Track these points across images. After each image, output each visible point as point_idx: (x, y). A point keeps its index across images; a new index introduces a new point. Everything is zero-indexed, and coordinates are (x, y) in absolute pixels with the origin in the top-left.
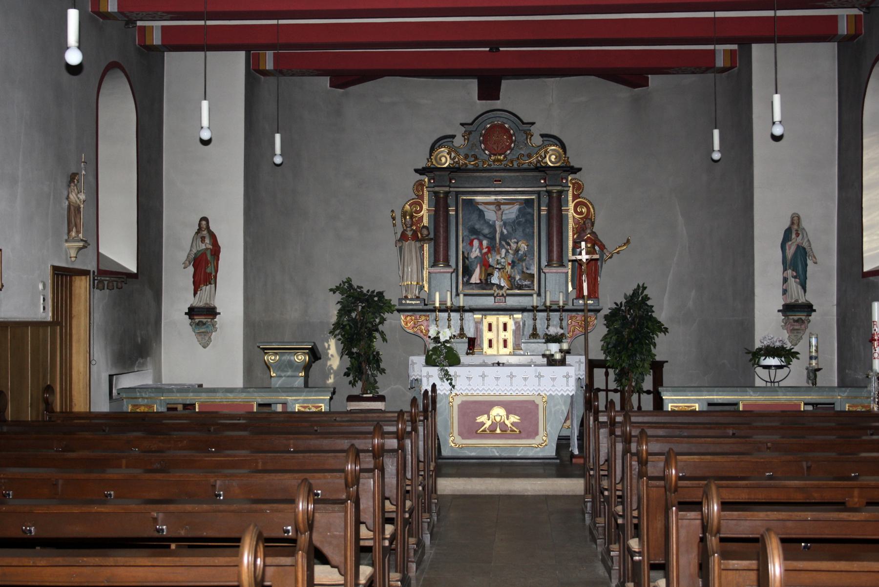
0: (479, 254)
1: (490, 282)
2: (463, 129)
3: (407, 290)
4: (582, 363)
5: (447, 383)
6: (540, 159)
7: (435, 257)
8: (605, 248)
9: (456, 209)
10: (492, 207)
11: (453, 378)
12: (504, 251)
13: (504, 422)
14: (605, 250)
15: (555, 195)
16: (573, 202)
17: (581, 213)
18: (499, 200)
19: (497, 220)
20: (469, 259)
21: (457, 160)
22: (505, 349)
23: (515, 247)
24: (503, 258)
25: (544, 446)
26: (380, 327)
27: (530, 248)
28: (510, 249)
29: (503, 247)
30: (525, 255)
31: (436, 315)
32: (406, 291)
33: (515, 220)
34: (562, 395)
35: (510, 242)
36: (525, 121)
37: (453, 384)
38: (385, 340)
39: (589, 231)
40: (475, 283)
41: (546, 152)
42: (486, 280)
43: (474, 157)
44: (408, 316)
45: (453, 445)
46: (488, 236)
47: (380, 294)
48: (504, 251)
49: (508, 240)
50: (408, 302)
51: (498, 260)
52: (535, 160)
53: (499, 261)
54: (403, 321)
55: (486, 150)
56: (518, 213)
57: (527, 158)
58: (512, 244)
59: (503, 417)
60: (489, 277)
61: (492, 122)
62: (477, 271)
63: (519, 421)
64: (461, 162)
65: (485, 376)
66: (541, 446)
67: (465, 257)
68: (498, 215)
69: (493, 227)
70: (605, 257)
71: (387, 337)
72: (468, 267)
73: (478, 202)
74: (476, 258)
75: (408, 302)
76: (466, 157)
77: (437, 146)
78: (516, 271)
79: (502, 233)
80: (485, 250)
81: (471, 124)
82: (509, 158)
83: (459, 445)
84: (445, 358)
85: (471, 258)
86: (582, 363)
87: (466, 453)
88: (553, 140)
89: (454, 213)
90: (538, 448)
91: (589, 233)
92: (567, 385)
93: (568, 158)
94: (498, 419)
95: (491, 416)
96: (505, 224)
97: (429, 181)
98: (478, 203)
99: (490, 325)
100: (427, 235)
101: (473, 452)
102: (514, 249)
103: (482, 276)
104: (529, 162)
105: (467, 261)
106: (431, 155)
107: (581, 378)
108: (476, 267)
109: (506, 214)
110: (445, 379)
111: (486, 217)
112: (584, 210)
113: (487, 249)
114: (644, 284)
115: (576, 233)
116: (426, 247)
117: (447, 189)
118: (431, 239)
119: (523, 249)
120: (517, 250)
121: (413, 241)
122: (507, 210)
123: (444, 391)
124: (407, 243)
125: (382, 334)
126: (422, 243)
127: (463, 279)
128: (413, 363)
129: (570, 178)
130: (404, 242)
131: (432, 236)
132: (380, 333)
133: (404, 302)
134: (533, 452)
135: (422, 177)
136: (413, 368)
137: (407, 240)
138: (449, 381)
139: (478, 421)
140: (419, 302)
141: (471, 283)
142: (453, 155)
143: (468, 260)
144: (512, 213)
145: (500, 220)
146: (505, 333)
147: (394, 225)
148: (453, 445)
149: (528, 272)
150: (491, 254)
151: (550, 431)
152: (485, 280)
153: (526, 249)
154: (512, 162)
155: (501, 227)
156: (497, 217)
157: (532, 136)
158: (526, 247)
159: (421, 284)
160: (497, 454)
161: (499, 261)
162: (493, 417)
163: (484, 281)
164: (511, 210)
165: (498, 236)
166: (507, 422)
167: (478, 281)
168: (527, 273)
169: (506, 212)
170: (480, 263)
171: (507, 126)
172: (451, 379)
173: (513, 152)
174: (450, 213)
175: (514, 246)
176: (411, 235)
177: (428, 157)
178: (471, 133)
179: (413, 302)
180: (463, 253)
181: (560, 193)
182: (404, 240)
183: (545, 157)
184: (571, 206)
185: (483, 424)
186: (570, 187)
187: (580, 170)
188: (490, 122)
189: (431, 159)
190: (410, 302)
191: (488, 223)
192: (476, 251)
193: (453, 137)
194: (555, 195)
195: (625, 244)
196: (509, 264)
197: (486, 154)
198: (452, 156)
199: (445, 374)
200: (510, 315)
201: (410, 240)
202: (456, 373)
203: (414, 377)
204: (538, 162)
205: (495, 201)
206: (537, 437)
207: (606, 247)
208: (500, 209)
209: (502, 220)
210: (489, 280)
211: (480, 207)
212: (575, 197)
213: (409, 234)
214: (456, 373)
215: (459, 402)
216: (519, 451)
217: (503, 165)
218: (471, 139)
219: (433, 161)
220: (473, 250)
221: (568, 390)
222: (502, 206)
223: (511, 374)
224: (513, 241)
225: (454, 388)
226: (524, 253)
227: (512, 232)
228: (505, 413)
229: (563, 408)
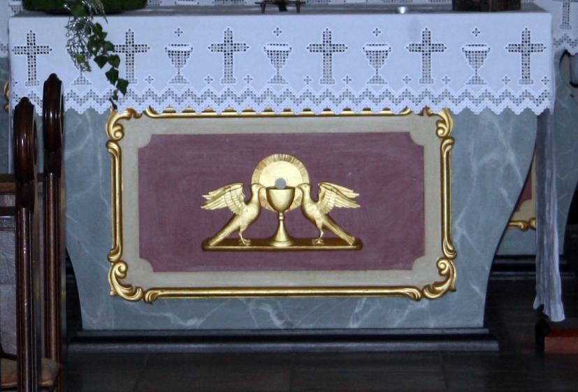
13: (302, 208)
25: (445, 293)
45: (121, 291)
59: (298, 193)
63: (355, 206)
65: (235, 47)
83: (144, 293)
94: (281, 197)
95: (255, 189)
101: (191, 317)
123: (91, 103)
134: (407, 312)
139: (211, 206)
148: (121, 291)
151: (463, 237)
160: (278, 324)
162: (264, 193)
185: (227, 216)
228: (307, 180)
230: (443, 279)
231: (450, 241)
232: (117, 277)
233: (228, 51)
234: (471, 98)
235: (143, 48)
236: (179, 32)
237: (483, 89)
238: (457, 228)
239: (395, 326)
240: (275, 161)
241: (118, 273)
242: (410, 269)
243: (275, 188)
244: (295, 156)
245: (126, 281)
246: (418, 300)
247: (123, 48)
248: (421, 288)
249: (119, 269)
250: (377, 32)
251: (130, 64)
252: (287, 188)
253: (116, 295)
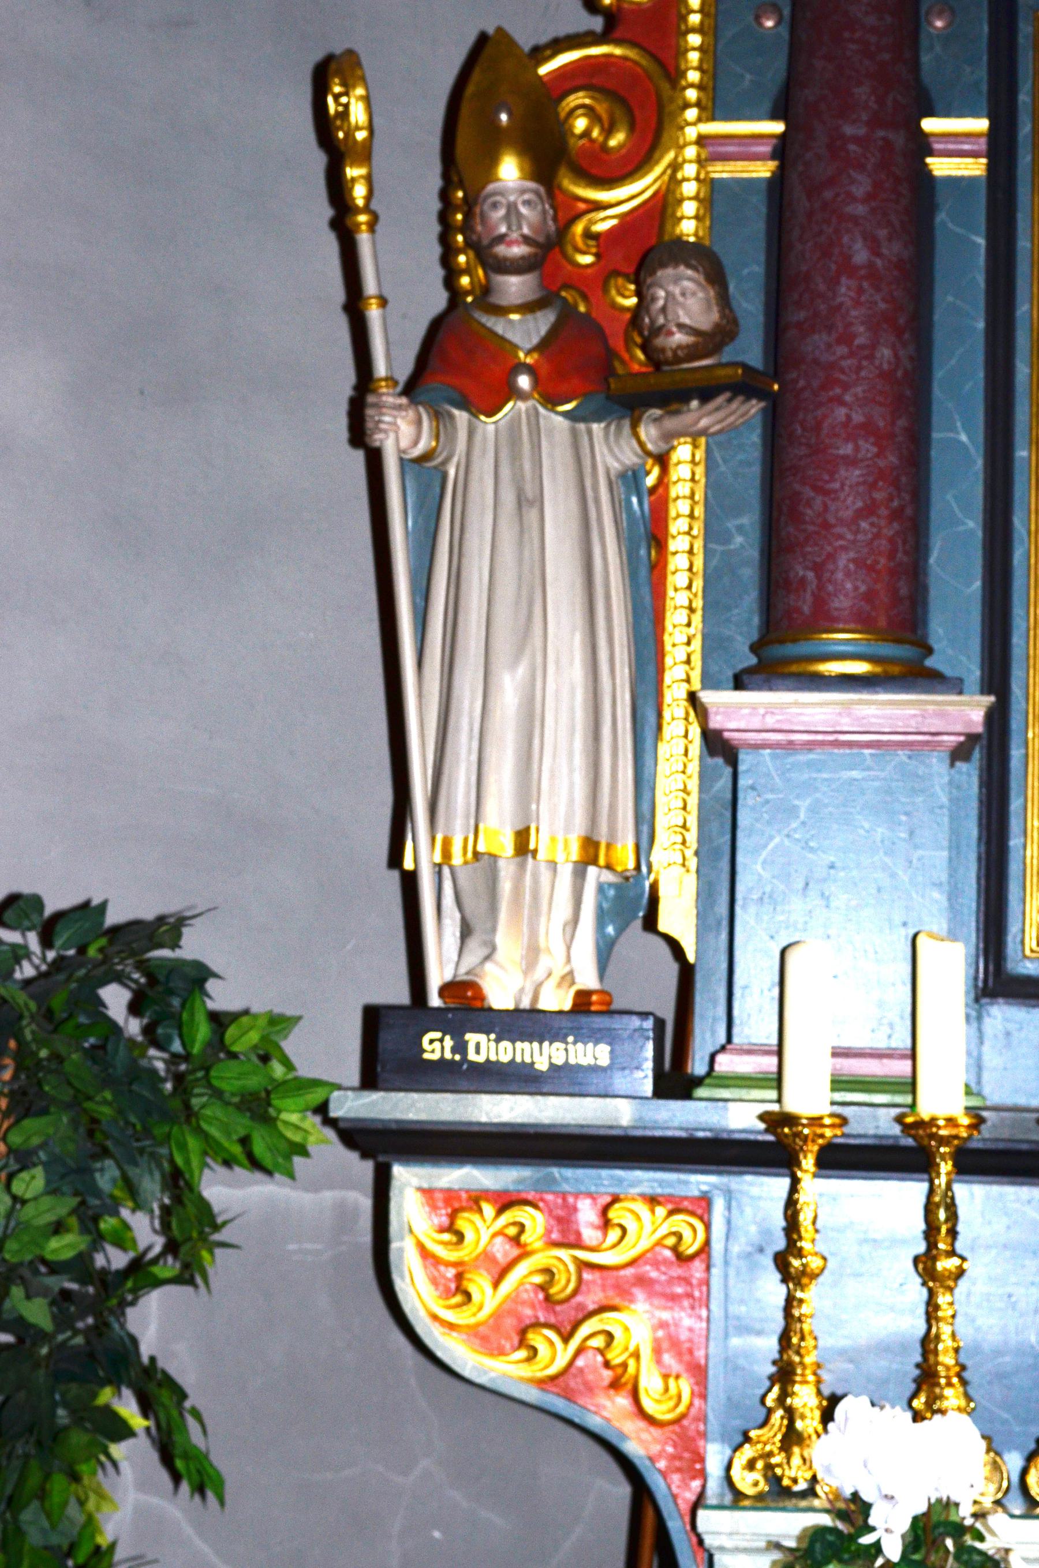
3: (475, 906)
31: (791, 1206)
32: (466, 931)
44: (475, 1200)
54: (425, 1253)
89: (974, 168)
121: (551, 401)
124: (488, 425)
126: (648, 432)
130: (461, 416)
159: (625, 857)
176: (542, 346)
182: (463, 406)
190: (504, 1052)
201: (522, 396)
213: (514, 336)
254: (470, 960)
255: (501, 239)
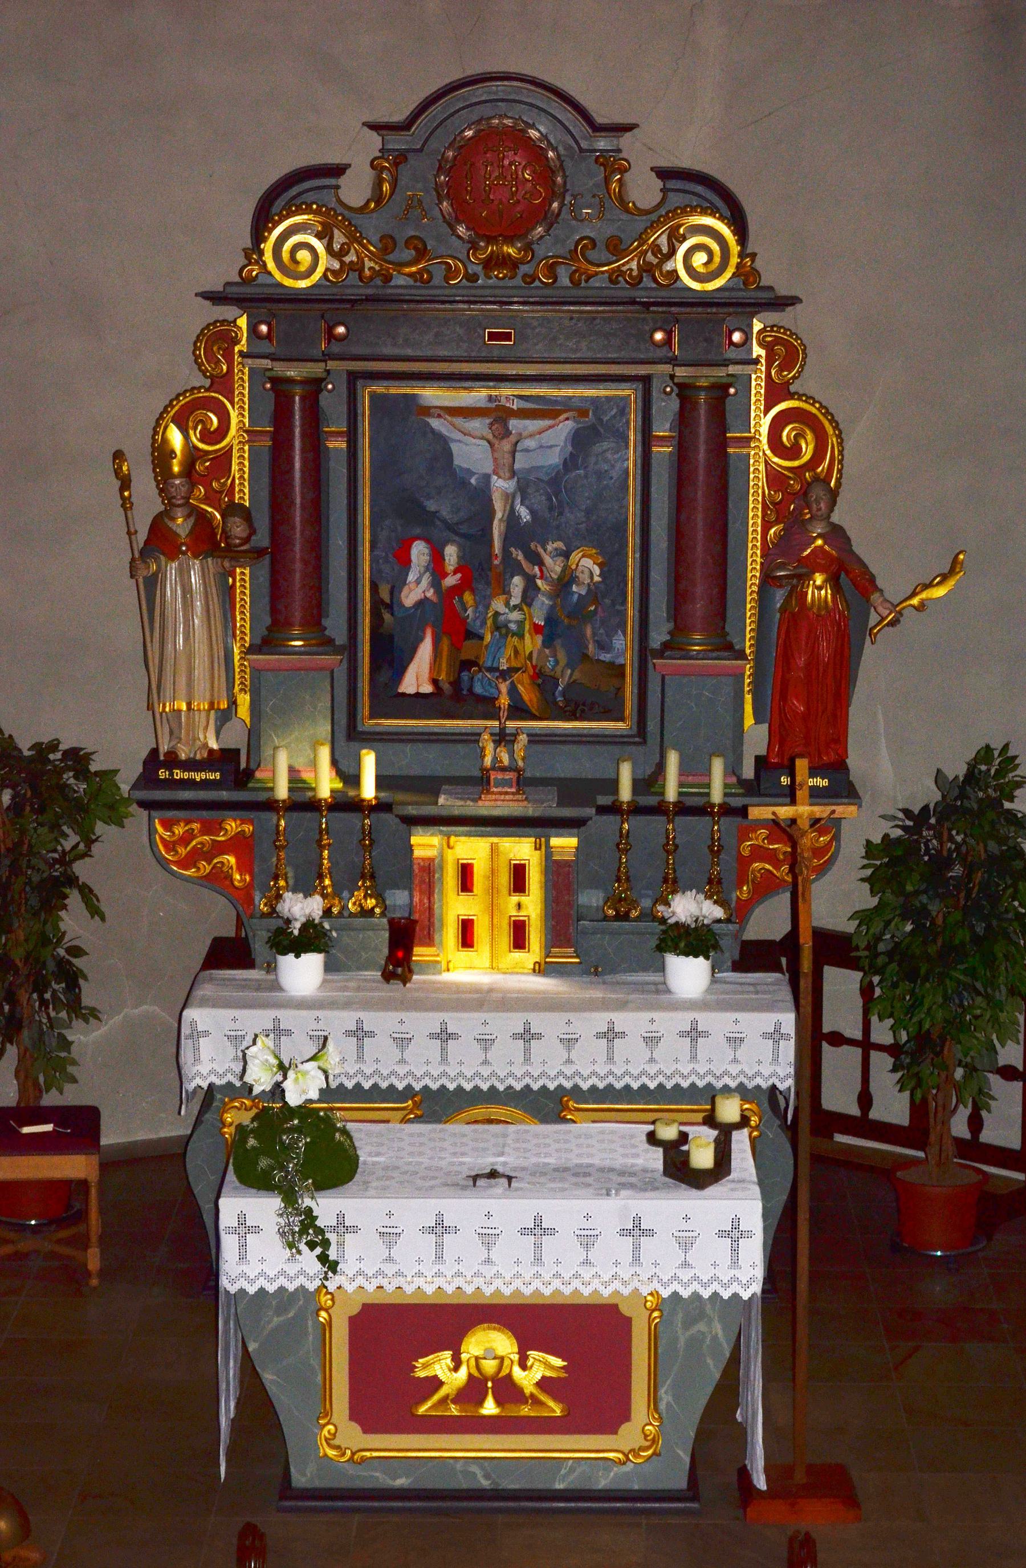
0: (430, 594)
1: (470, 690)
2: (375, 141)
3: (174, 726)
4: (785, 1037)
5: (309, 1260)
6: (655, 261)
7: (274, 611)
8: (877, 589)
9: (349, 431)
10: (478, 425)
11: (332, 1237)
12: (517, 583)
13: (509, 1376)
14: (875, 597)
15: (702, 397)
16: (766, 412)
17: (793, 452)
18: (503, 402)
19: (495, 472)
20: (395, 608)
21: (351, 258)
22: (518, 955)
23: (558, 569)
24: (515, 607)
25: (650, 1457)
26: (81, 869)
27: (613, 568)
28: (541, 578)
29: (518, 570)
30: (594, 594)
32: (171, 733)
33: (558, 473)
34: (715, 1295)
35: (540, 550)
36: (600, 120)
37: (333, 1254)
38: (95, 911)
39: (818, 529)
40: (418, 695)
41: (676, 238)
42: (456, 684)
43: (416, 249)
45: (331, 1453)
46: (464, 529)
47: (77, 758)
48: (517, 583)
49: (532, 545)
50: (179, 774)
51: (497, 614)
52: (634, 265)
53: (502, 618)
55: (459, 221)
56: (570, 448)
57: (605, 256)
58: (548, 560)
59: (507, 1362)
60: (465, 676)
61: (479, 122)
62: (425, 650)
63: (563, 1375)
64: (368, 264)
65: (446, 1230)
66: (637, 1456)
67: (382, 602)
68: (496, 455)
69: (482, 495)
70: (874, 618)
71: (104, 907)
72: (391, 637)
73: (430, 408)
74: (421, 603)
75: (179, 774)
76: (388, 244)
77: (280, 203)
78: (562, 657)
79: (512, 517)
80: (451, 581)
81: (406, 126)
82: (540, 250)
83: (353, 1454)
84: (304, 1172)
85: (401, 605)
86: (785, 1037)
87: (377, 1478)
88: (699, 189)
90: (630, 1466)
91: (820, 536)
92: (735, 1263)
93: (753, 256)
94: (489, 1366)
95: (464, 1357)
96: (523, 489)
97: (253, 329)
98: (427, 411)
99: (466, 872)
100: (246, 540)
101: (400, 1477)
102: (555, 577)
103: (439, 673)
104: (613, 270)
105: (387, 616)
106: (258, 236)
107: (782, 1087)
108: (421, 639)
109: (527, 450)
110: (303, 1247)
111: (457, 462)
112: (808, 450)
113: (459, 575)
114: (1006, 747)
115: (777, 522)
116: (243, 576)
117: (316, 369)
118: (260, 553)
119: (586, 571)
120: (565, 581)
122: (531, 436)
123: (301, 1281)
125: (87, 893)
127: (372, 680)
128: (196, 1035)
129: (757, 326)
131: (262, 539)
132: (81, 891)
133: (163, 774)
134: (612, 1474)
135: (227, 312)
136: (196, 1049)
137: (173, 553)
138: (318, 1250)
139: (421, 1374)
140: (218, 776)
141: (404, 695)
142: (339, 239)
143: (392, 614)
144: (551, 447)
145: (507, 475)
146: (515, 899)
147: (126, 505)
148: (331, 1453)
149: (606, 657)
150: (473, 591)
151: (668, 1404)
152: (451, 683)
153: (597, 579)
154: (551, 270)
155: (510, 498)
156: (495, 460)
157: (623, 171)
158: (597, 570)
160: (485, 1484)
161: (502, 618)
162: (473, 1362)
163: (446, 687)
164: (548, 437)
165: (497, 530)
166: (518, 1373)
167: (427, 688)
168: (598, 661)
169: (530, 443)
170: (433, 627)
171: (533, 133)
172: (326, 1244)
173: (556, 230)
174: (331, 445)
175: (554, 566)
177: (249, 244)
178: (406, 158)
179: (198, 777)
180: (374, 588)
181: (720, 389)
183: (672, 252)
184: (762, 424)
185: (436, 1383)
186: (756, 361)
187: (792, 301)
188: (475, 118)
189: (261, 253)
190: (186, 776)
191: (464, 483)
192: (418, 582)
193: (338, 170)
194: (702, 397)
195: (945, 578)
196: (537, 629)
197: (459, 237)
198: (336, 247)
199: (303, 1231)
200: (538, 837)
202: (341, 1217)
203: (198, 1081)
204: (647, 269)
205: (493, 405)
206: (625, 1429)
207: (879, 582)
208: (507, 433)
209: (513, 473)
210: (465, 685)
211: (435, 423)
212: (775, 393)
213: (180, 531)
214: (341, 1217)
215: (355, 1428)
216: (563, 1472)
217: (519, 278)
218: (403, 182)
219: (268, 258)
220: (411, 577)
221: (735, 1279)
222: (514, 424)
223: (538, 1220)
224: (550, 547)
225: (335, 1272)
226: (589, 591)
227: (547, 515)
228: (516, 1350)
229: (718, 1328)
230: (648, 1444)
231: (656, 1409)
232: (326, 1440)
233: (439, 1228)
234: (680, 1282)
235: (354, 1229)
236: (390, 1214)
237: (691, 1273)
238: (663, 1396)
239: (600, 1487)
240: (484, 1330)
241: (327, 1436)
242: (616, 1433)
243: (485, 1358)
244: (504, 1325)
245: (336, 1442)
246: (624, 1463)
247: (334, 1229)
248: (626, 1452)
249: (329, 1432)
250: (587, 1217)
251: (341, 1244)
252: (495, 1358)
253: (326, 1455)
254: (173, 743)
255: (174, 497)
